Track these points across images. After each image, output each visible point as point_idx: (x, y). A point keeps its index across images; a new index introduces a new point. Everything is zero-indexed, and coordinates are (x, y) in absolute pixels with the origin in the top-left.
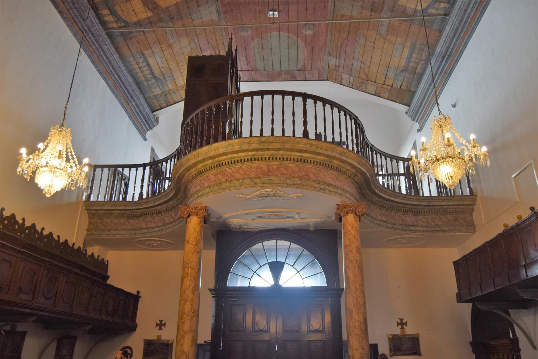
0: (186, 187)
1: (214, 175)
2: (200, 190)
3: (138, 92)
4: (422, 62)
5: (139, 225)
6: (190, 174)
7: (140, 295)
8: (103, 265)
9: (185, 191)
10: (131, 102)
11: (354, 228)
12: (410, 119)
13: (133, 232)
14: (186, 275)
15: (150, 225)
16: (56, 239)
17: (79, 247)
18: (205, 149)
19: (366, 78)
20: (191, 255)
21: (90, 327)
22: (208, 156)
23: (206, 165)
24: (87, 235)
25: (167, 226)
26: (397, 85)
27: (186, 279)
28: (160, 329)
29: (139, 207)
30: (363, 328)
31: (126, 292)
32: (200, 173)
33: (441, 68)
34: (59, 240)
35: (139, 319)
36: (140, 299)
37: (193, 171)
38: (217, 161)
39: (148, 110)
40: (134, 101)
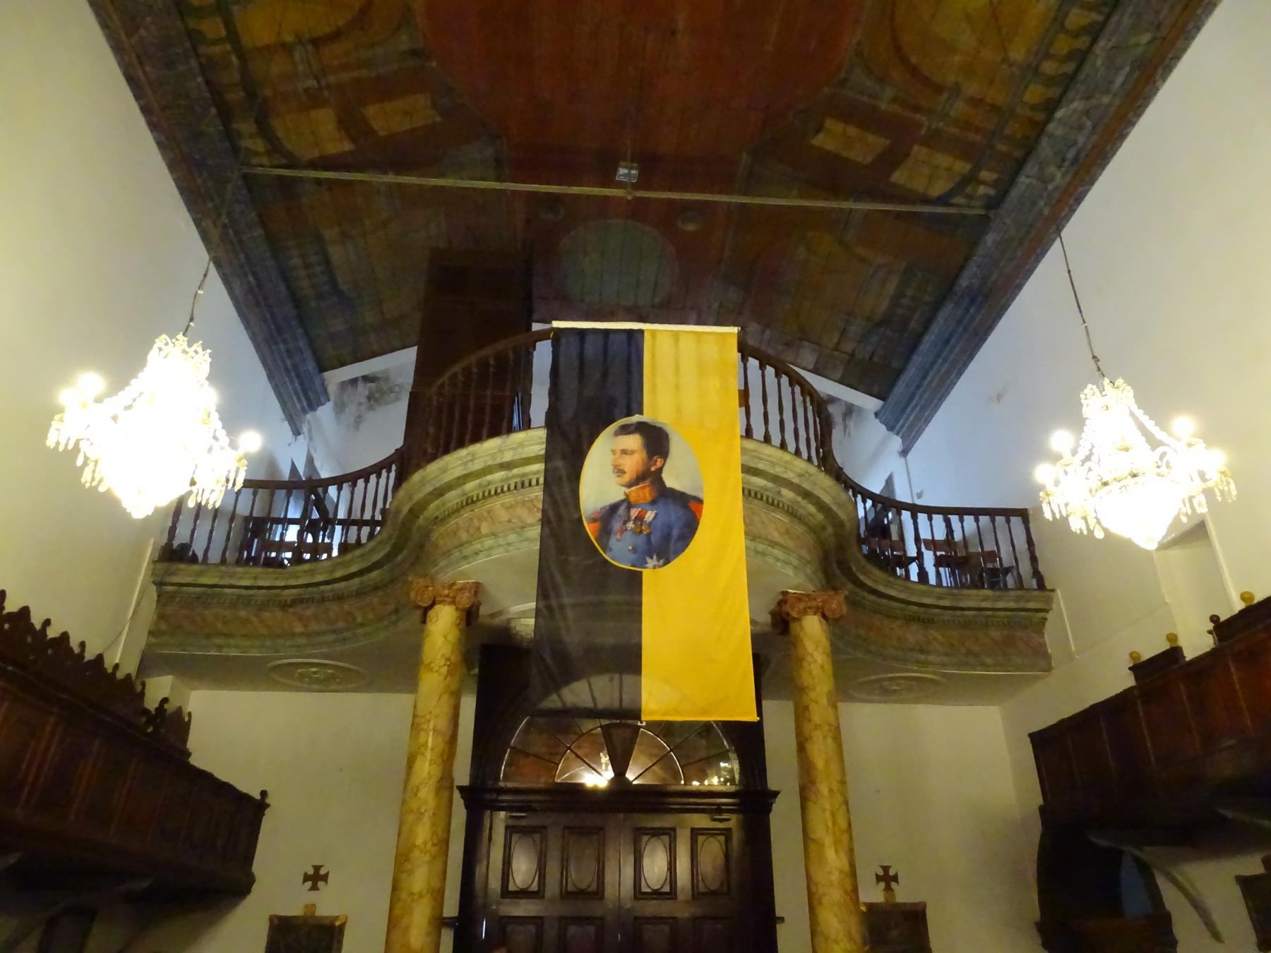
0: (427, 534)
2: (469, 542)
6: (444, 504)
7: (267, 801)
9: (421, 546)
11: (821, 650)
14: (422, 749)
15: (314, 627)
16: (77, 650)
17: (129, 676)
18: (492, 444)
22: (499, 461)
23: (489, 483)
24: (148, 645)
25: (360, 631)
29: (292, 582)
30: (849, 888)
32: (470, 502)
36: (267, 811)
37: (453, 497)
39: (311, 365)
40: (285, 341)
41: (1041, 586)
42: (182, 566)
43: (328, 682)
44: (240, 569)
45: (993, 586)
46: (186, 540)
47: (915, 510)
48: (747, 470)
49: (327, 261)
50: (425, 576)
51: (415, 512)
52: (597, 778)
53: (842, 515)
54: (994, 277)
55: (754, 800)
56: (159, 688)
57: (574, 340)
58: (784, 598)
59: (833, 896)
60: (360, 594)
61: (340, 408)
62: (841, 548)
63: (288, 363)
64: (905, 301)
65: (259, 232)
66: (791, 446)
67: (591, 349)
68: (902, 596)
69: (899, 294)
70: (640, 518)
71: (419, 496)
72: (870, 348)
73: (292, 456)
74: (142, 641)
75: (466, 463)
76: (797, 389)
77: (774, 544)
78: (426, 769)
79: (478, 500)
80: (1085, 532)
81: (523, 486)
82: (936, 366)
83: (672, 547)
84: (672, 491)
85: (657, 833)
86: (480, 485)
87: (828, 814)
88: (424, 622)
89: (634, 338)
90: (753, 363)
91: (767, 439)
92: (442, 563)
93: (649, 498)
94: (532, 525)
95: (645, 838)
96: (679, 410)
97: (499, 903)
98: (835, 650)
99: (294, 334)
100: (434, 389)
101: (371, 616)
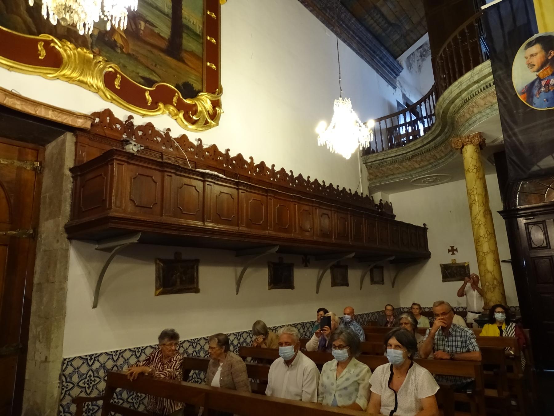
0: (453, 119)
1: (483, 99)
5: (412, 166)
9: (453, 124)
10: (375, 58)
13: (408, 174)
15: (422, 164)
18: (467, 75)
21: (393, 258)
22: (472, 81)
23: (472, 92)
25: (440, 161)
27: (474, 206)
28: (453, 254)
29: (408, 150)
32: (466, 101)
34: (351, 193)
37: (458, 102)
38: (482, 85)
39: (391, 59)
40: (377, 55)
42: (370, 156)
43: (435, 182)
44: (390, 151)
49: (382, 15)
50: (457, 136)
56: (378, 197)
60: (436, 147)
61: (410, 66)
70: (547, 84)
71: (444, 106)
73: (395, 97)
74: (367, 183)
75: (459, 87)
78: (478, 209)
79: (469, 100)
81: (487, 87)
86: (468, 94)
92: (462, 129)
93: (550, 73)
99: (380, 50)
101: (443, 155)
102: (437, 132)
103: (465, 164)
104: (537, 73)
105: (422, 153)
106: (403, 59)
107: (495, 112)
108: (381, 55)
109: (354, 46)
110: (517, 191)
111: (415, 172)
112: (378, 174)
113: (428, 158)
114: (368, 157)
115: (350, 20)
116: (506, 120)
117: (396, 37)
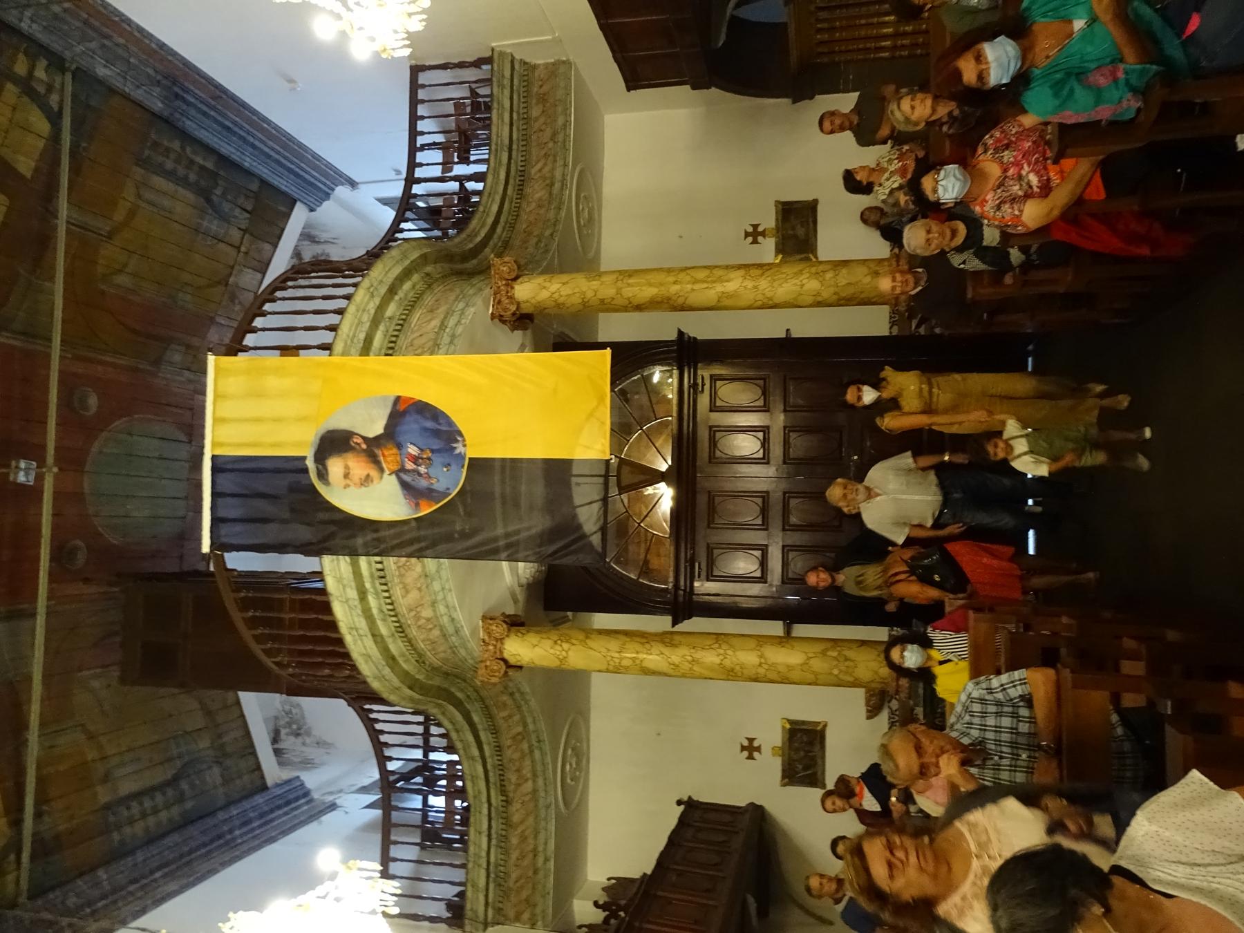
0: (435, 669)
1: (407, 592)
2: (442, 628)
3: (210, 822)
4: (188, 150)
5: (527, 798)
6: (403, 655)
7: (686, 799)
8: (619, 886)
9: (447, 674)
11: (547, 284)
12: (326, 204)
13: (543, 813)
14: (638, 662)
15: (527, 772)
18: (338, 610)
19: (221, 288)
20: (592, 652)
21: (751, 900)
22: (357, 603)
23: (382, 611)
24: (545, 927)
25: (531, 727)
26: (243, 219)
27: (645, 664)
28: (758, 749)
29: (484, 799)
30: (758, 272)
31: (677, 826)
32: (401, 629)
33: (205, 108)
35: (739, 800)
37: (396, 647)
38: (373, 583)
39: (259, 799)
40: (231, 831)
41: (488, 61)
42: (468, 906)
43: (579, 754)
44: (472, 849)
45: (488, 108)
46: (442, 905)
47: (411, 180)
48: (366, 350)
49: (137, 796)
50: (475, 670)
51: (413, 684)
52: (664, 496)
53: (415, 255)
54: (151, 72)
55: (686, 353)
57: (224, 529)
58: (498, 317)
59: (765, 286)
60: (495, 731)
61: (308, 764)
62: (449, 257)
63: (255, 824)
64: (181, 171)
65: (102, 874)
66: (341, 303)
67: (232, 509)
68: (498, 198)
69: (170, 175)
70: (415, 460)
71: (396, 682)
72: (237, 211)
73: (358, 809)
75: (360, 636)
76: (279, 294)
77: (443, 326)
78: (654, 657)
80: (425, 17)
82: (257, 143)
83: (444, 428)
84: (387, 427)
85: (713, 443)
86: (384, 620)
87: (696, 287)
88: (521, 667)
89: (219, 466)
90: (250, 340)
91: (333, 328)
93: (395, 451)
94: (424, 566)
95: (718, 454)
96: (303, 419)
97: (771, 585)
98: (549, 271)
100: (283, 673)
101: (517, 718)
102: (459, 717)
103: (545, 663)
104: (387, 472)
105: (501, 768)
106: (272, 771)
107: (444, 574)
108: (237, 823)
109: (172, 886)
110: (637, 581)
111: (542, 794)
112: (524, 894)
113: (516, 756)
114: (468, 913)
115: (97, 884)
116: (463, 550)
117: (214, 775)
